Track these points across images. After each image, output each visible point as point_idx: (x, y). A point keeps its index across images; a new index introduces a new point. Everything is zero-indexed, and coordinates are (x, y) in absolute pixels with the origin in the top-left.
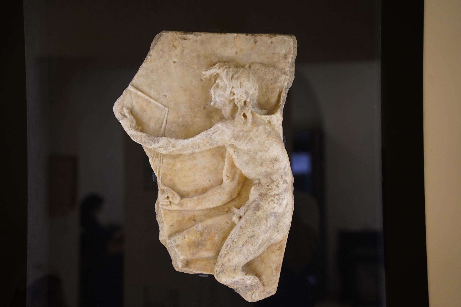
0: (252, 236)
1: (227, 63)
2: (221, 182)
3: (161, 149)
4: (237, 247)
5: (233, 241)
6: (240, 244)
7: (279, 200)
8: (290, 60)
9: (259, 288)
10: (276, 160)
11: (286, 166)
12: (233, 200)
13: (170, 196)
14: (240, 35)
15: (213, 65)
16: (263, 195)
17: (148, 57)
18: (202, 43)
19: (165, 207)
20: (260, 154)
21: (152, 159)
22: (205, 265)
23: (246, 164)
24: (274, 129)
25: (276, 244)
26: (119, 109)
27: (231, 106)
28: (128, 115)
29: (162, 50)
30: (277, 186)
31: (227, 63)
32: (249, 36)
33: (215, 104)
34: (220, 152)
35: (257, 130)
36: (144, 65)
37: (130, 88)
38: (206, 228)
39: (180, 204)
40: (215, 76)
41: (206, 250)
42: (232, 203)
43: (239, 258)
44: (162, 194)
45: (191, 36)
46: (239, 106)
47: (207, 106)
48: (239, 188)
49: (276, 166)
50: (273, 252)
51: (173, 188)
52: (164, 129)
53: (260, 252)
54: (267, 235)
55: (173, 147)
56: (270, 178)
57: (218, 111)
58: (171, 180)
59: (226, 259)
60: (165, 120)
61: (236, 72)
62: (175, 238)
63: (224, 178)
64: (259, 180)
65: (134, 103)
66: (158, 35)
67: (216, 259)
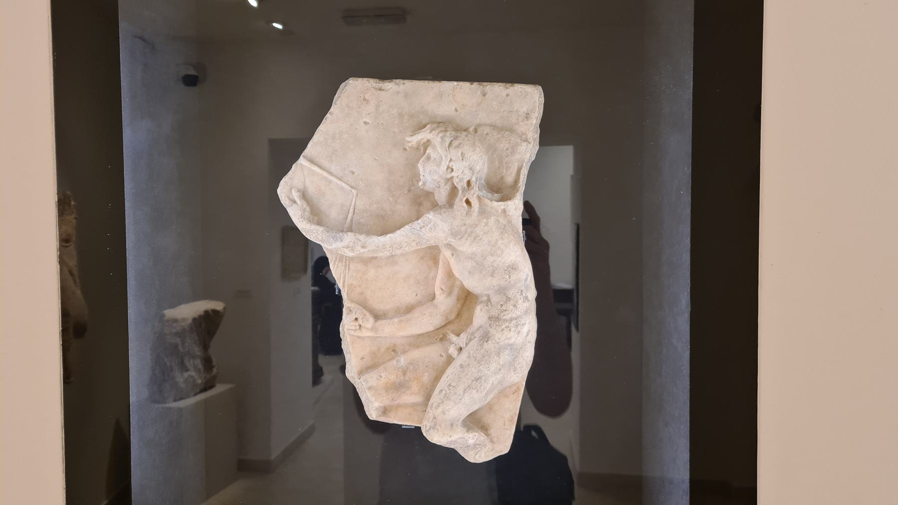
0: (477, 379)
1: (442, 124)
2: (433, 297)
3: (346, 251)
4: (455, 394)
5: (450, 385)
6: (460, 389)
7: (517, 326)
8: (535, 122)
9: (485, 446)
10: (513, 268)
11: (528, 276)
12: (449, 323)
13: (360, 317)
14: (461, 83)
15: (421, 127)
16: (495, 319)
17: (328, 115)
18: (406, 95)
19: (352, 333)
20: (490, 259)
21: (334, 264)
22: (410, 414)
23: (470, 272)
24: (510, 222)
25: (510, 387)
26: (287, 190)
27: (448, 187)
28: (298, 202)
29: (348, 106)
30: (515, 306)
31: (442, 124)
32: (475, 85)
33: (424, 184)
34: (432, 254)
35: (486, 224)
36: (322, 127)
37: (302, 160)
38: (411, 363)
39: (373, 329)
40: (424, 144)
41: (411, 394)
42: (448, 327)
43: (459, 410)
44: (348, 314)
45: (391, 86)
46: (460, 188)
47: (413, 188)
48: (459, 306)
49: (514, 277)
50: (506, 396)
51: (364, 305)
52: (351, 221)
53: (489, 399)
54: (499, 376)
55: (363, 247)
56: (505, 294)
57: (429, 195)
58: (362, 293)
59: (440, 410)
60: (352, 207)
61: (456, 138)
62: (366, 376)
63: (438, 292)
64: (488, 296)
65: (308, 183)
66: (343, 84)
67: (426, 405)
